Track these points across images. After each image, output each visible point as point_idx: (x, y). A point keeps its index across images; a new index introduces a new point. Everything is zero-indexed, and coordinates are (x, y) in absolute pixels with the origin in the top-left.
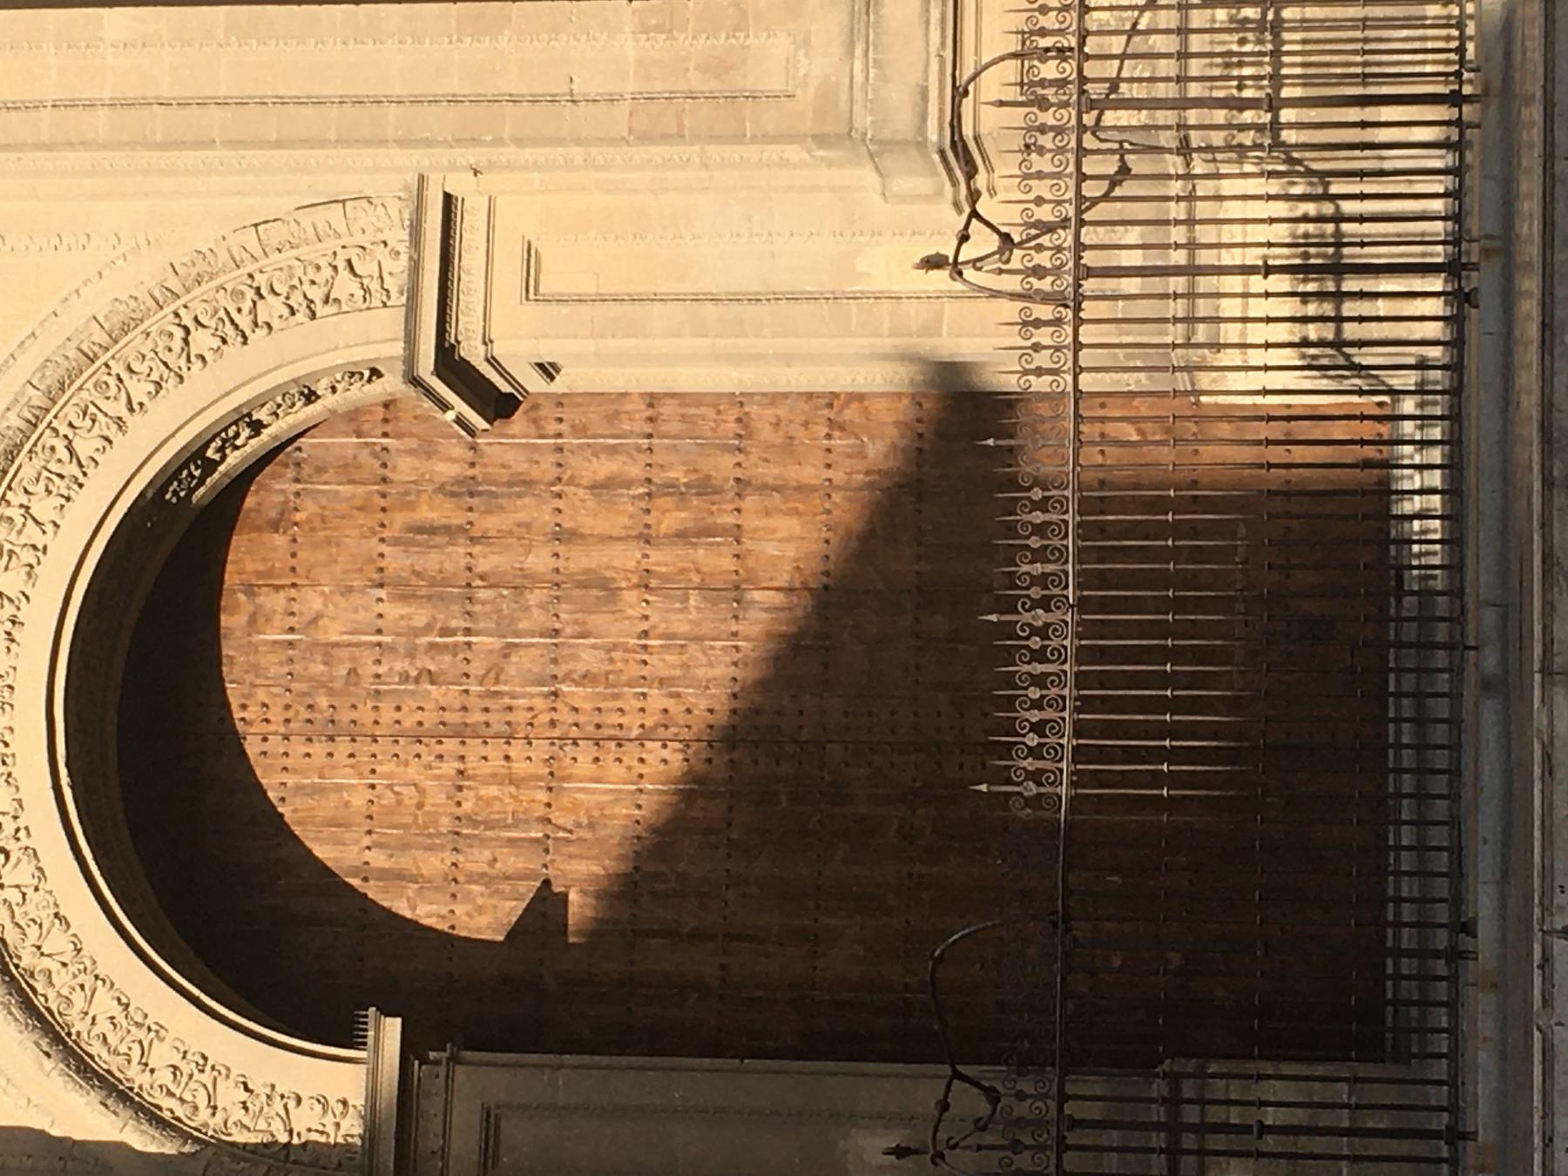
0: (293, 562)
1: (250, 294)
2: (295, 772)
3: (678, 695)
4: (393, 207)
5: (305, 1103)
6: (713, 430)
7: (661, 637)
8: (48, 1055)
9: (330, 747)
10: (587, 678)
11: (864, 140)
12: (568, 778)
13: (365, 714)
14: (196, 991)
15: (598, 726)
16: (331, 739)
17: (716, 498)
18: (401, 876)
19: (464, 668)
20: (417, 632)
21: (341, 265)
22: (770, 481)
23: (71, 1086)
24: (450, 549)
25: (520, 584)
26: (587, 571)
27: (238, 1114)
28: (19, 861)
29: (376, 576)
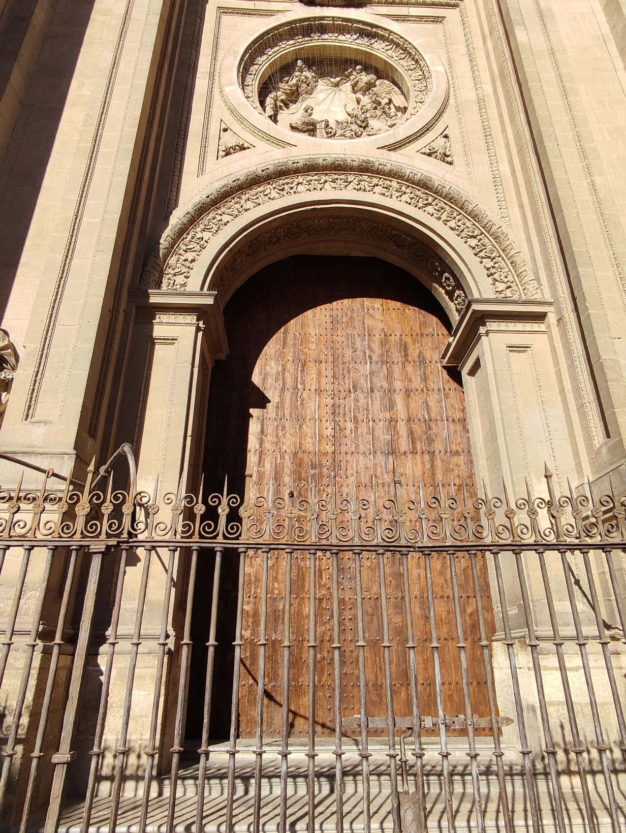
0: (391, 309)
1: (493, 256)
2: (320, 312)
3: (351, 433)
5: (186, 280)
6: (452, 442)
7: (373, 426)
8: (208, 197)
9: (329, 321)
13: (339, 333)
14: (231, 246)
18: (285, 345)
20: (370, 348)
22: (435, 464)
25: (389, 377)
27: (182, 258)
28: (279, 194)
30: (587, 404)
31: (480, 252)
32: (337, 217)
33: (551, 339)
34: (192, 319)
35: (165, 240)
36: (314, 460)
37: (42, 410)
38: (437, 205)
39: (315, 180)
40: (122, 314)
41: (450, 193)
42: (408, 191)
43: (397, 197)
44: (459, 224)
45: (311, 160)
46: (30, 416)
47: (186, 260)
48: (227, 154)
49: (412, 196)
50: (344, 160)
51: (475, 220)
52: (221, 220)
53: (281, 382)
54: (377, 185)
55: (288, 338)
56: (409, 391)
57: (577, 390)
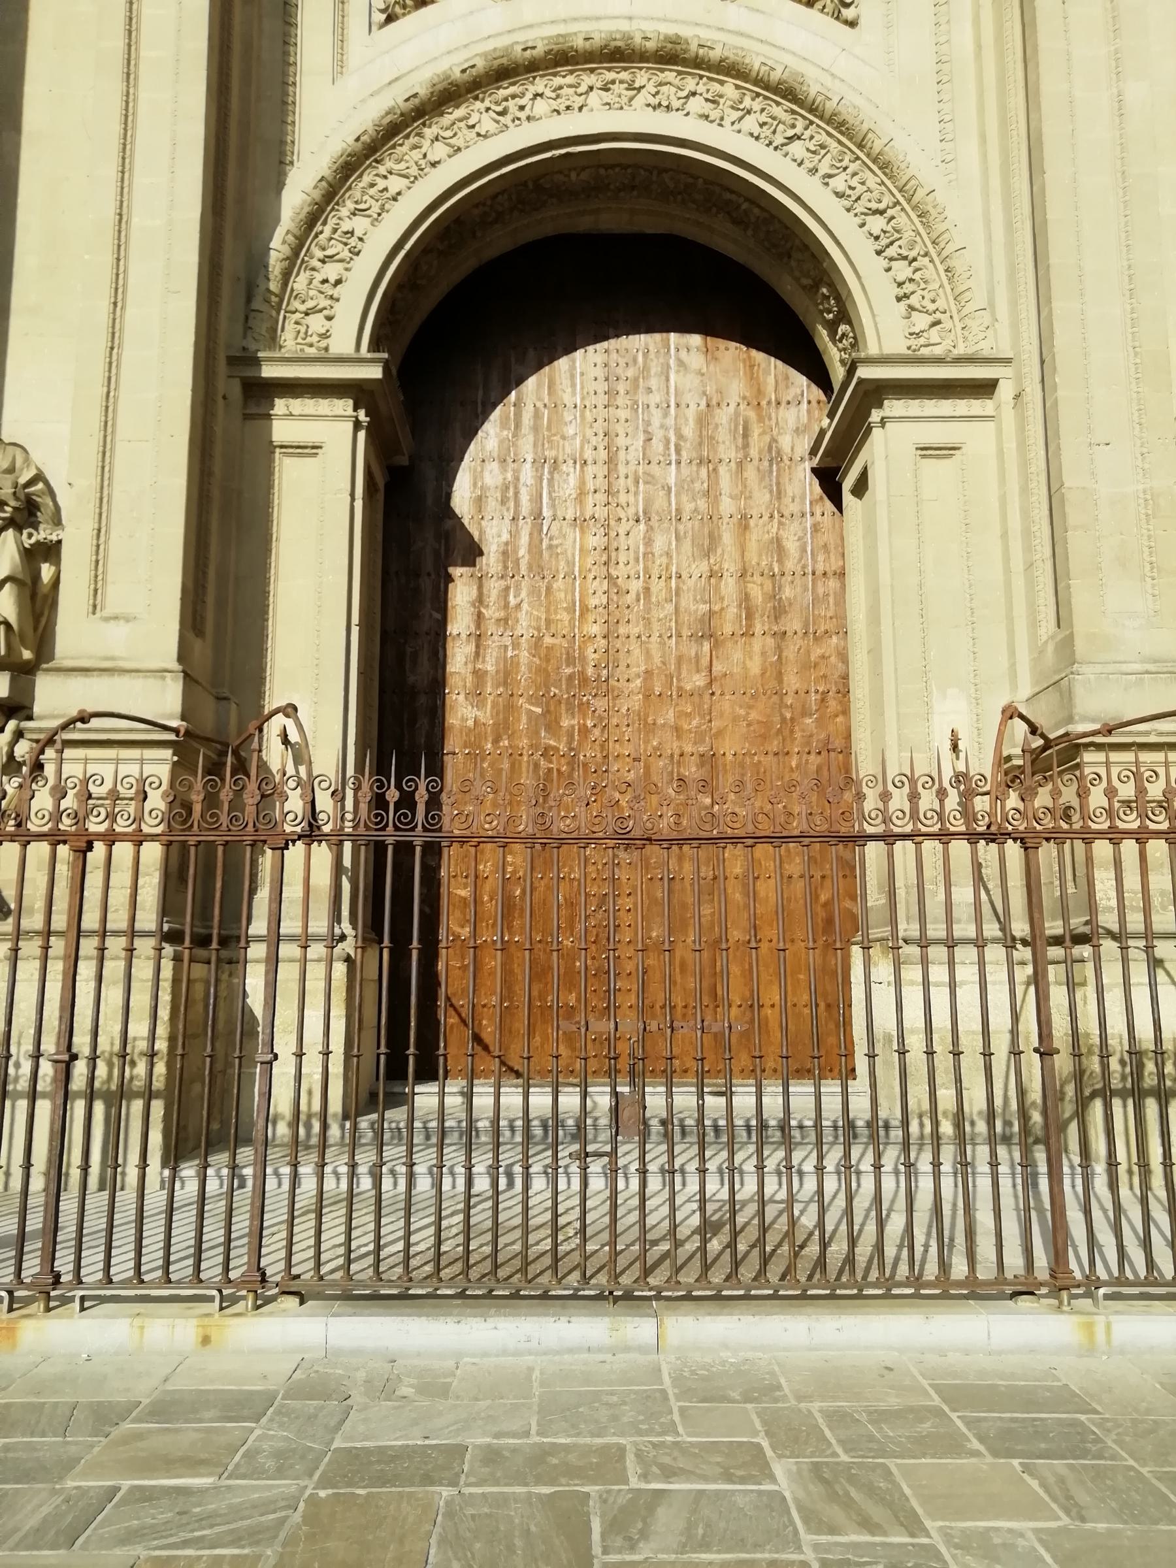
3: (638, 600)
4: (982, 345)
5: (328, 324)
8: (357, 139)
9: (601, 377)
10: (649, 542)
11: (1072, 673)
12: (582, 531)
14: (408, 246)
15: (617, 549)
16: (607, 379)
17: (772, 618)
19: (655, 461)
21: (938, 315)
23: (335, 156)
24: (733, 447)
25: (711, 494)
26: (720, 537)
27: (319, 277)
28: (497, 122)
29: (714, 402)
30: (1039, 563)
31: (888, 246)
32: (613, 167)
33: (999, 431)
34: (344, 406)
35: (284, 242)
36: (571, 651)
37: (115, 597)
38: (812, 138)
39: (570, 86)
40: (220, 401)
41: (840, 113)
42: (757, 105)
43: (733, 123)
44: (854, 182)
45: (561, 40)
46: (98, 607)
47: (325, 281)
48: (390, 19)
49: (763, 118)
50: (628, 37)
51: (885, 174)
52: (386, 189)
53: (512, 504)
54: (694, 94)
55: (524, 413)
56: (746, 518)
57: (1027, 534)
